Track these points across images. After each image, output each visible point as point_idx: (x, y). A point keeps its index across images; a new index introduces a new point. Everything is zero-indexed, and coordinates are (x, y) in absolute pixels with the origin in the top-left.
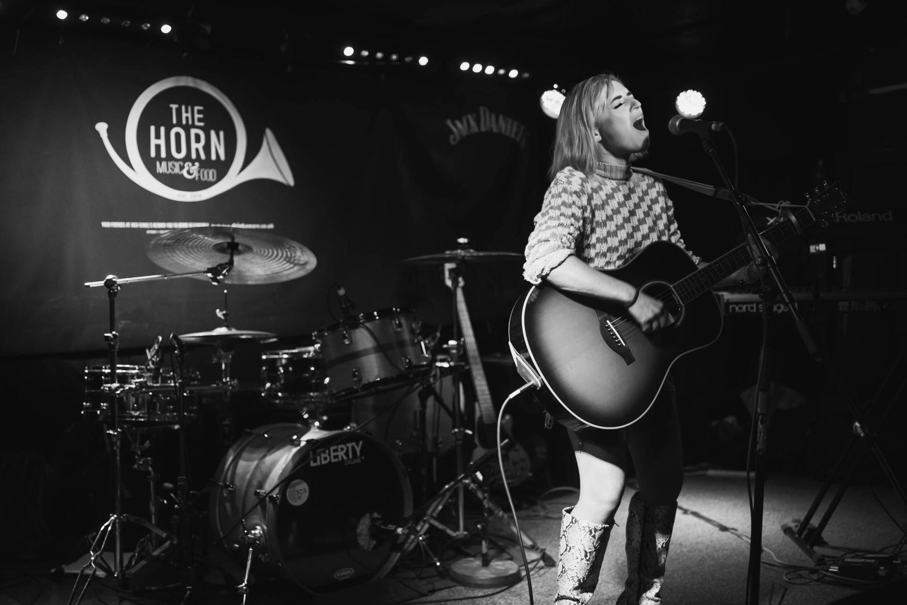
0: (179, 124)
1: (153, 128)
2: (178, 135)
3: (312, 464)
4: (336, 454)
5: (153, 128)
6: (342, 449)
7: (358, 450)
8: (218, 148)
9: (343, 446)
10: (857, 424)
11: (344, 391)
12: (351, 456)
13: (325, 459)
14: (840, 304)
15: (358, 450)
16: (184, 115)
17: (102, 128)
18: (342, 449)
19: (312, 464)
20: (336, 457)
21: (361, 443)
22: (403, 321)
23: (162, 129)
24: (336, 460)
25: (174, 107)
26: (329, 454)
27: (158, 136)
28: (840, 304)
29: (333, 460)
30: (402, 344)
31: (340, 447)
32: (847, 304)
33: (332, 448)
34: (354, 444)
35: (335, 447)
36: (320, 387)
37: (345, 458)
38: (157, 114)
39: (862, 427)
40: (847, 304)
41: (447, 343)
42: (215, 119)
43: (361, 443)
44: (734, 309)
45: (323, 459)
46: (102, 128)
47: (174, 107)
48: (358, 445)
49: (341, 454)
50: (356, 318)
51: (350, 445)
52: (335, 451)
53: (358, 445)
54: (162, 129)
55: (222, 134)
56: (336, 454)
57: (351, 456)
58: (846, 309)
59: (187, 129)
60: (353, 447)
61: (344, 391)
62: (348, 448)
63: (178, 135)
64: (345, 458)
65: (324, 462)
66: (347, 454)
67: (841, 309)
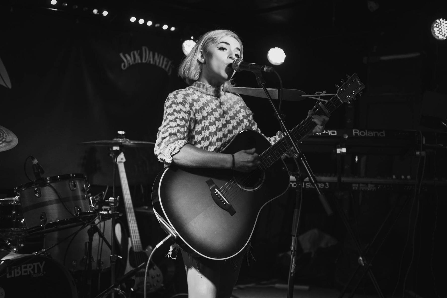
3: (8, 276)
4: (25, 270)
6: (30, 267)
7: (42, 267)
9: (31, 265)
10: (361, 258)
11: (34, 228)
12: (36, 272)
13: (18, 273)
14: (354, 185)
15: (42, 267)
18: (30, 267)
19: (8, 276)
20: (25, 272)
21: (44, 262)
22: (78, 183)
24: (26, 274)
26: (21, 270)
28: (354, 185)
29: (23, 274)
30: (76, 198)
31: (29, 265)
32: (357, 185)
33: (23, 266)
34: (39, 263)
35: (25, 265)
36: (18, 224)
37: (32, 273)
39: (363, 260)
40: (357, 185)
41: (108, 199)
43: (44, 262)
44: (291, 185)
45: (16, 273)
48: (41, 264)
49: (29, 270)
50: (45, 180)
51: (35, 264)
52: (25, 267)
53: (41, 264)
56: (25, 270)
57: (36, 272)
58: (357, 188)
60: (38, 265)
61: (34, 228)
62: (34, 266)
64: (32, 273)
65: (16, 275)
66: (33, 270)
67: (354, 188)
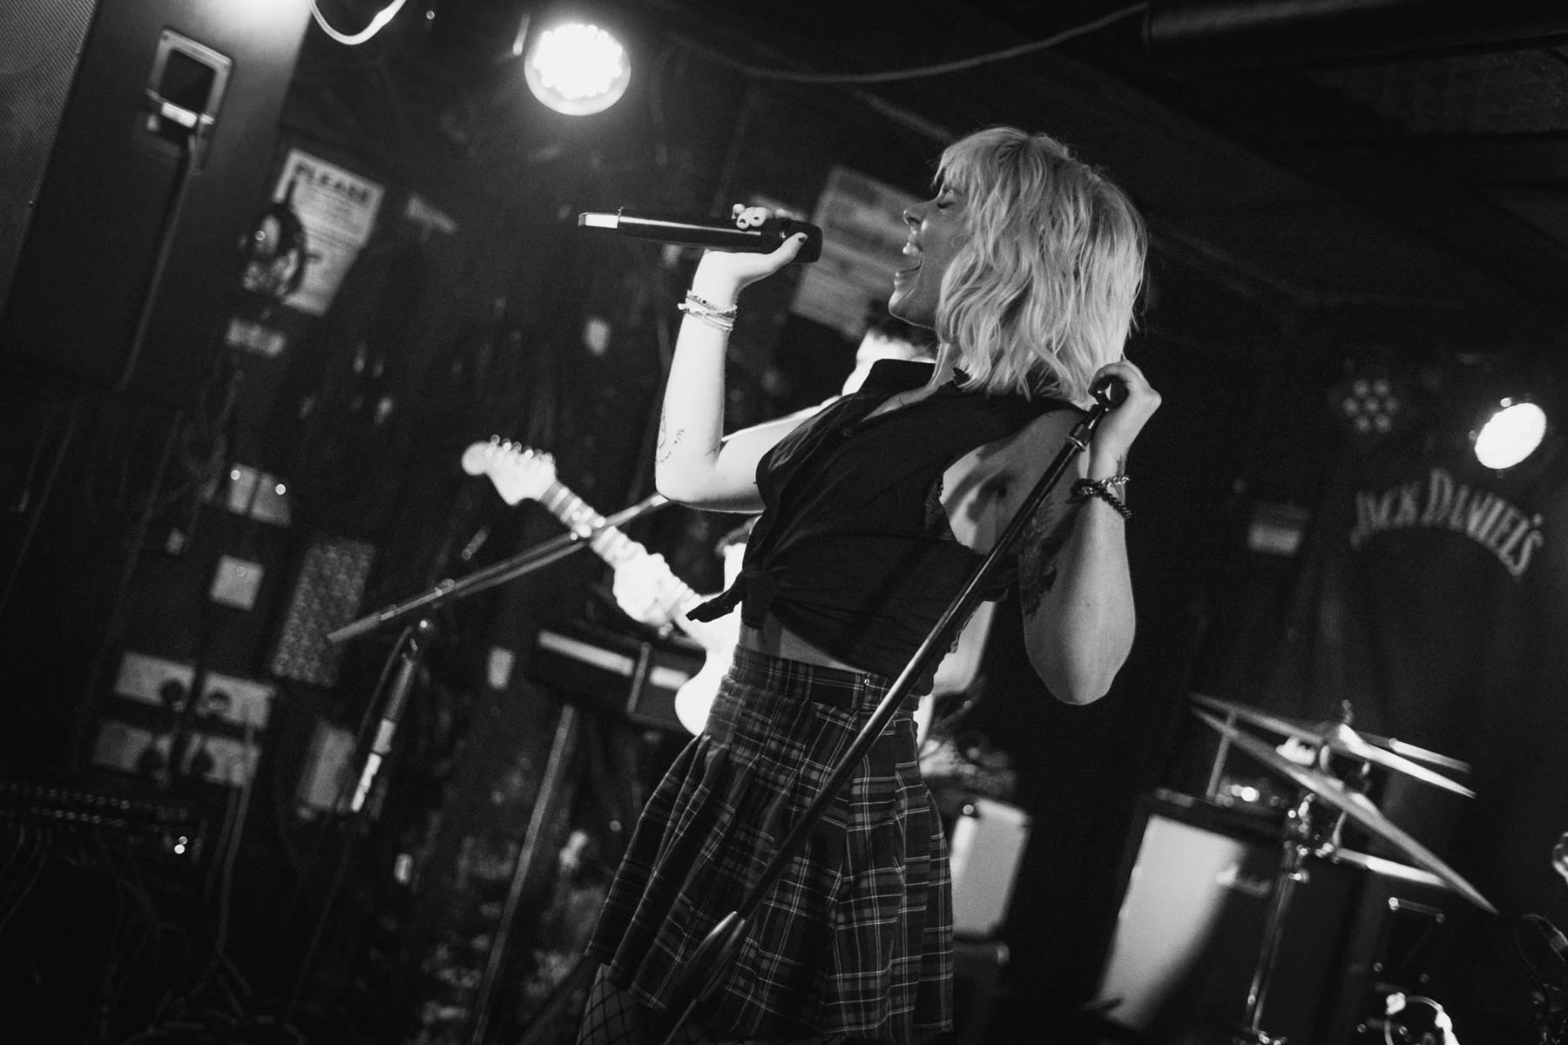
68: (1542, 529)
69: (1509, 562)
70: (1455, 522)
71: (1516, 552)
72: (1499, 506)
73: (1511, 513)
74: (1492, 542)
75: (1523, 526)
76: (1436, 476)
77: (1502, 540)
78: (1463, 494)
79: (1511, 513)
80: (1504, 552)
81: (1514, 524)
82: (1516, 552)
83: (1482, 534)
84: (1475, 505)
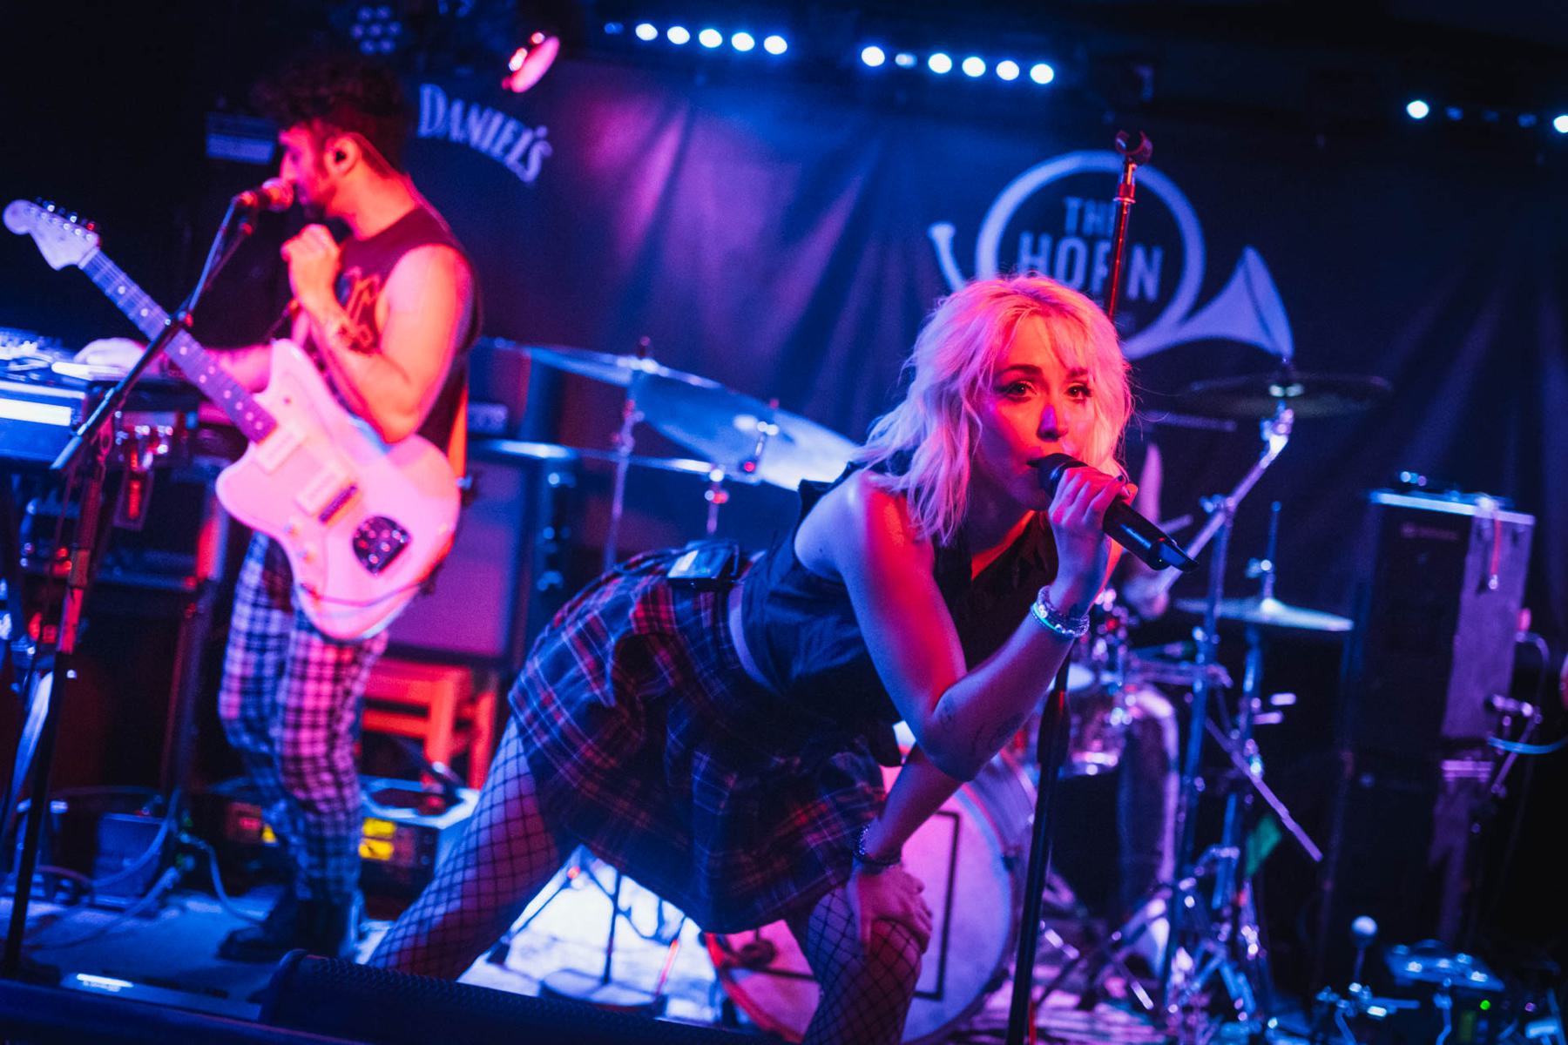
0: (1079, 233)
1: (1026, 241)
2: (1072, 254)
5: (1026, 241)
8: (1143, 274)
16: (1092, 218)
17: (942, 234)
23: (1045, 242)
25: (1073, 204)
27: (1035, 251)
38: (1041, 216)
42: (1150, 225)
46: (942, 234)
47: (1073, 204)
54: (1045, 242)
55: (1157, 255)
59: (1091, 241)
63: (1072, 254)
68: (548, 138)
69: (518, 169)
70: (456, 134)
71: (524, 159)
72: (497, 120)
73: (511, 126)
74: (497, 150)
75: (526, 138)
76: (426, 92)
77: (508, 149)
78: (457, 108)
79: (511, 126)
80: (512, 159)
81: (517, 136)
82: (524, 159)
83: (486, 144)
84: (473, 117)
